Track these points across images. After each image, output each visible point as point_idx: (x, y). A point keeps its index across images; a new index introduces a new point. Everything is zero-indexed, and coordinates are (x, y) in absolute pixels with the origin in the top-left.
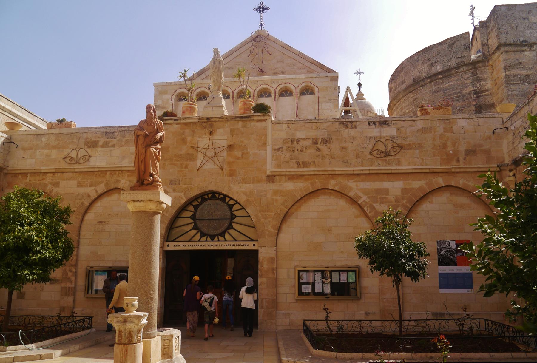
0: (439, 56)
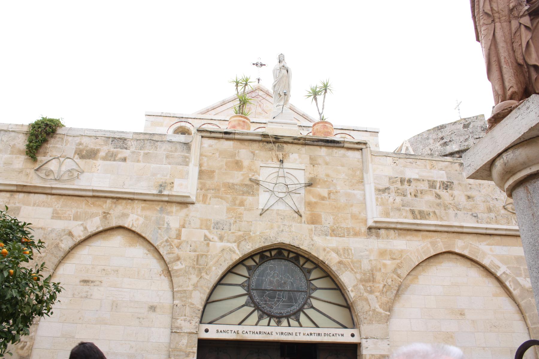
0: (453, 135)
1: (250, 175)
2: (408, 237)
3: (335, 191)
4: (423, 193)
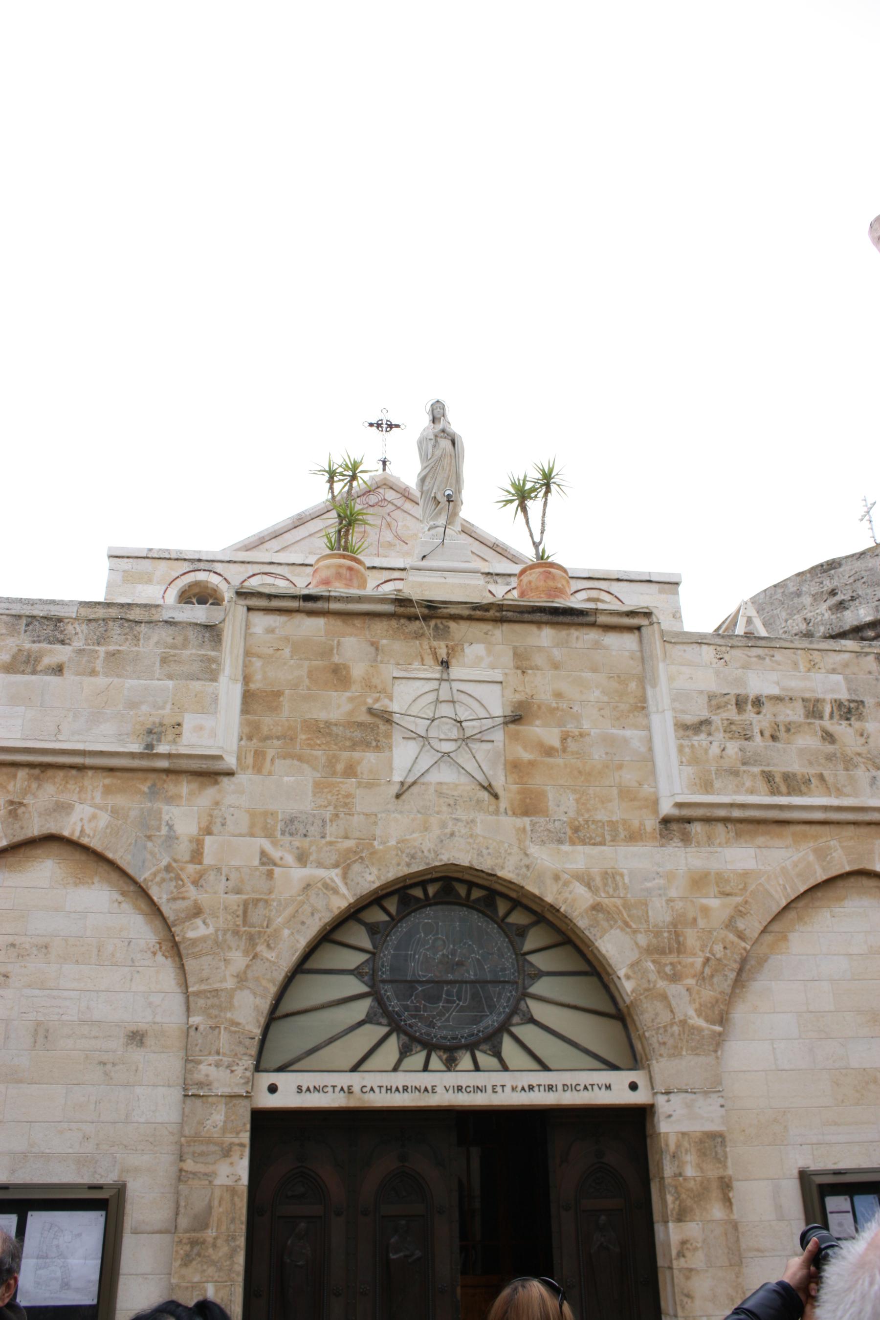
0: (859, 584)
1: (370, 701)
2: (761, 840)
3: (577, 734)
4: (793, 731)
